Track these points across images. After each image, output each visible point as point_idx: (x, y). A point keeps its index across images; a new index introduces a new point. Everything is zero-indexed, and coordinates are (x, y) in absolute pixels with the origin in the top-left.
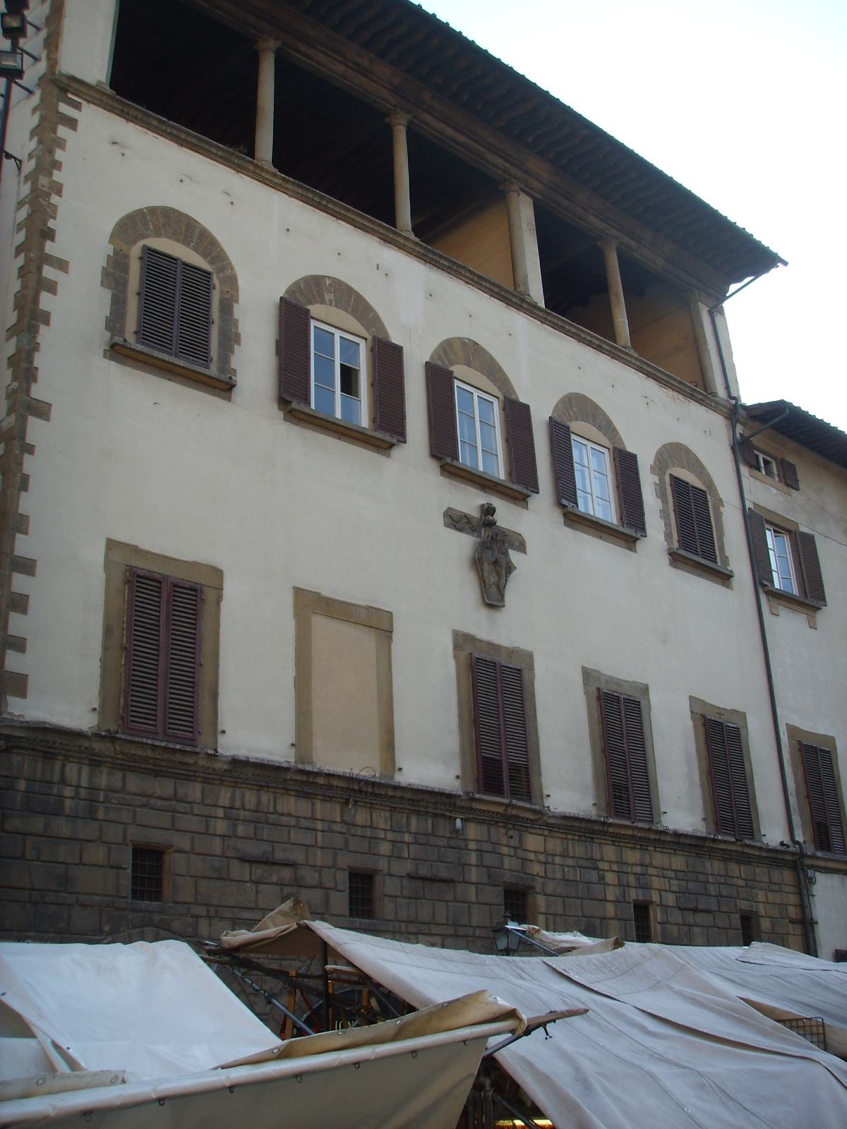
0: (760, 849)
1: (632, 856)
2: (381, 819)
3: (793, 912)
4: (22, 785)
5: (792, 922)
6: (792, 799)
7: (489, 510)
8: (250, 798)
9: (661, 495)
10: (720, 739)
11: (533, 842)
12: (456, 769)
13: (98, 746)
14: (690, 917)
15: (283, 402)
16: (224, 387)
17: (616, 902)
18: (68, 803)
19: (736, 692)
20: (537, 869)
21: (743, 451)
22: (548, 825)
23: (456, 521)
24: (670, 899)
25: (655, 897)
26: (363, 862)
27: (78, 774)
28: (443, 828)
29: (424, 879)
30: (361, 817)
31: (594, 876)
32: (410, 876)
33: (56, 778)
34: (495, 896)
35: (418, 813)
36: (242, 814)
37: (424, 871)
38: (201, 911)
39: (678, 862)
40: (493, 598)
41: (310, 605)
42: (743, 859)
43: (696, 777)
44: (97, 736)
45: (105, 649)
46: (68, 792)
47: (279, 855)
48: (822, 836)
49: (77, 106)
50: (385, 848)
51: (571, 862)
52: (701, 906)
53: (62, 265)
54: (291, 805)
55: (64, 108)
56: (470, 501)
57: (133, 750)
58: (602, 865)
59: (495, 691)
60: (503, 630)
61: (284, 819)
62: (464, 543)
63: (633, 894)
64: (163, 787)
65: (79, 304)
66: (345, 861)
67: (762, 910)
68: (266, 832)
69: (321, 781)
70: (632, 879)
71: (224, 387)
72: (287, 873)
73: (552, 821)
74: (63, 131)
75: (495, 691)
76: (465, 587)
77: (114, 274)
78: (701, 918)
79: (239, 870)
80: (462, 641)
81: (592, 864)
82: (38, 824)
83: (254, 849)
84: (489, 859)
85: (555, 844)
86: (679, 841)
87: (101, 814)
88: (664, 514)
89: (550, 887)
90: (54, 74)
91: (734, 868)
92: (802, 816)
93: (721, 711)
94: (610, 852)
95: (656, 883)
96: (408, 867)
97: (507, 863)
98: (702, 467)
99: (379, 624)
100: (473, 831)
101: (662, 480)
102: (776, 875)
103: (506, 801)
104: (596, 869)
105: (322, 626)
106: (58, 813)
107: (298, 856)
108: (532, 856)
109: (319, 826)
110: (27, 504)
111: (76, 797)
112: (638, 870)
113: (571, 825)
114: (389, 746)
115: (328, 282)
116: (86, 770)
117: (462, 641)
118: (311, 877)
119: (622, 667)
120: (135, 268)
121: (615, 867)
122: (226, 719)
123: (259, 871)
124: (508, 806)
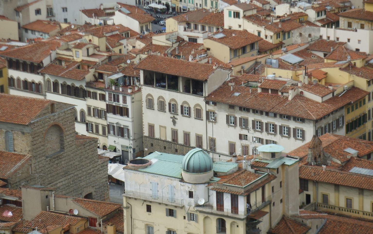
1: (187, 148)
6: (208, 145)
8: (157, 141)
9: (194, 110)
11: (178, 146)
19: (202, 132)
20: (178, 148)
23: (171, 118)
26: (165, 146)
30: (164, 143)
34: (174, 150)
41: (160, 126)
43: (195, 141)
53: (143, 101)
54: (160, 141)
56: (172, 116)
59: (175, 133)
62: (172, 120)
65: (144, 104)
75: (175, 133)
77: (146, 101)
80: (172, 129)
81: (183, 148)
85: (179, 146)
88: (194, 113)
94: (185, 147)
98: (201, 106)
99: (165, 128)
101: (194, 109)
105: (161, 128)
110: (143, 121)
117: (172, 129)
119: (187, 130)
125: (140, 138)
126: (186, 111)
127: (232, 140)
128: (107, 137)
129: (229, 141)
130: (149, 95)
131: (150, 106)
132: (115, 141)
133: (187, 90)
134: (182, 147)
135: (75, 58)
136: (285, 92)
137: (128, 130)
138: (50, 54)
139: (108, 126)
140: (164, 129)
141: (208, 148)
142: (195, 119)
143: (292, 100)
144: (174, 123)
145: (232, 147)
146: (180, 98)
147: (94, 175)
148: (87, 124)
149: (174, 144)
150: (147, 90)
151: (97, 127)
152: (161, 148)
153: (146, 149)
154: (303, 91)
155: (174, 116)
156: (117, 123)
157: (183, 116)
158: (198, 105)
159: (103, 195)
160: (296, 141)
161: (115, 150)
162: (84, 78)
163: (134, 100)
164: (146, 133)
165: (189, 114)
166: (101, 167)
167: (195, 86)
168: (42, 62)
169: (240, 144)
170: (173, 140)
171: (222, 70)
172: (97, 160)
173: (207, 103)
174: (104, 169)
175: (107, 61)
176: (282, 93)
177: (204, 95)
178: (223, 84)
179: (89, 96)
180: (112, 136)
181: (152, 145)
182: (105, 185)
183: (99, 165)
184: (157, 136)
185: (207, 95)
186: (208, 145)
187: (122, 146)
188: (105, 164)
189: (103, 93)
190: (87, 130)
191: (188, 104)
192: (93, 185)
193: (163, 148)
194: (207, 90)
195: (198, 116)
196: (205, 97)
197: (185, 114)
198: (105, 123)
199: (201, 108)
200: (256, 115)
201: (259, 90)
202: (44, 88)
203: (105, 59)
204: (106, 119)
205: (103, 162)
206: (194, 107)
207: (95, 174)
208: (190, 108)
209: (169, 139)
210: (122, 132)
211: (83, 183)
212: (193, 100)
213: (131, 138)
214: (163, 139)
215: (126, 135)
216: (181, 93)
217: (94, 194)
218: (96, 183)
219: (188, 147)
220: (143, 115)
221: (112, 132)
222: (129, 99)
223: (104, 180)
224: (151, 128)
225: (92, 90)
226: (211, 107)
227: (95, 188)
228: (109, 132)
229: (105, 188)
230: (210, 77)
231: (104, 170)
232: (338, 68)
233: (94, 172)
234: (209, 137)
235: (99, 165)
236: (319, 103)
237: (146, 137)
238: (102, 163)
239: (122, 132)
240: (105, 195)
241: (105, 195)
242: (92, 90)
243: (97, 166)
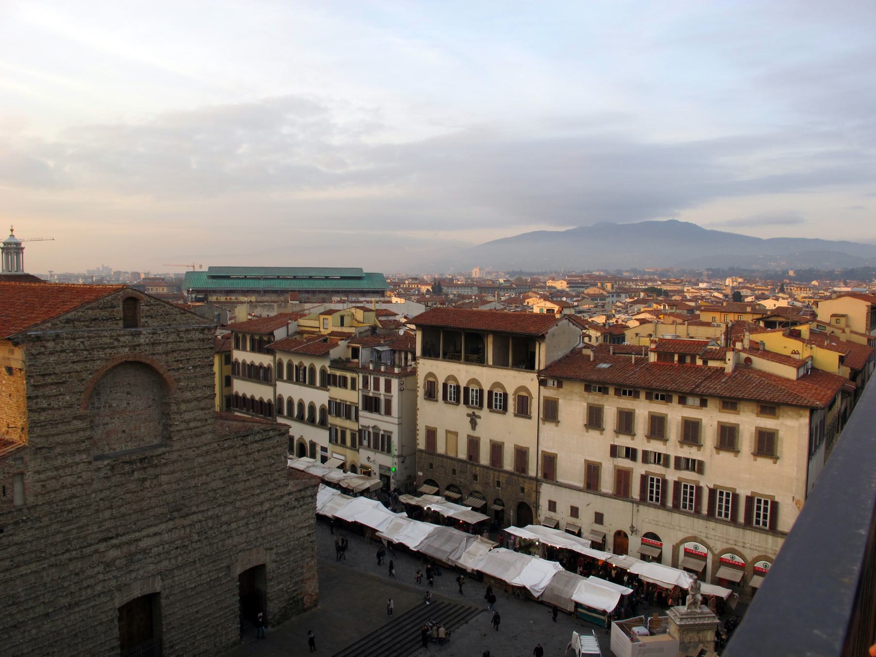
1: (497, 473)
9: (514, 400)
10: (521, 454)
11: (478, 468)
16: (437, 401)
23: (468, 415)
39: (506, 475)
41: (448, 432)
42: (523, 477)
48: (545, 476)
56: (470, 411)
59: (474, 444)
60: (475, 434)
65: (421, 392)
71: (437, 401)
75: (474, 444)
76: (469, 426)
80: (468, 436)
86: (506, 472)
88: (514, 405)
99: (456, 434)
105: (449, 435)
113: (484, 467)
117: (468, 436)
119: (498, 439)
125: (409, 455)
126: (497, 401)
128: (358, 451)
129: (586, 461)
130: (431, 374)
131: (430, 395)
132: (369, 458)
133: (501, 362)
135: (322, 330)
136: (714, 359)
138: (288, 324)
139: (360, 431)
140: (454, 437)
141: (539, 475)
142: (515, 415)
143: (734, 371)
144: (474, 425)
145: (592, 472)
146: (487, 376)
147: (273, 519)
148: (330, 429)
149: (472, 464)
150: (425, 367)
151: (343, 433)
153: (420, 474)
154: (752, 357)
155: (474, 413)
156: (374, 427)
157: (491, 411)
158: (523, 388)
159: (300, 570)
160: (755, 460)
161: (368, 473)
162: (328, 353)
163: (403, 386)
164: (422, 444)
165: (505, 409)
166: (296, 499)
167: (519, 348)
168: (272, 334)
169: (612, 467)
170: (470, 457)
171: (571, 324)
172: (283, 481)
173: (542, 383)
174: (304, 504)
175: (369, 333)
176: (705, 362)
177: (537, 368)
178: (572, 352)
179: (335, 385)
180: (365, 448)
181: (431, 466)
182: (306, 545)
183: (290, 494)
184: (441, 449)
185: (542, 368)
186: (540, 467)
187: (381, 467)
188: (309, 493)
189: (355, 375)
190: (330, 441)
191: (503, 387)
192: (268, 545)
193: (451, 473)
194: (542, 356)
195: (523, 410)
196: (540, 373)
197: (496, 407)
198: (354, 426)
199: (530, 394)
200: (654, 405)
201: (653, 358)
202: (274, 374)
203: (366, 331)
204: (357, 419)
205: (302, 487)
206: (515, 394)
207: (276, 516)
208: (505, 395)
209: (463, 455)
210: (381, 443)
211: (236, 540)
212: (513, 380)
214: (451, 454)
216: (490, 366)
217: (270, 567)
218: (277, 539)
219: (499, 471)
220: (418, 412)
221: (365, 443)
222: (395, 383)
223: (305, 532)
224: (431, 434)
225: (338, 373)
226: (548, 392)
227: (274, 551)
228: (361, 443)
229: (304, 553)
230: (550, 331)
231: (304, 507)
232: (818, 319)
233: (274, 511)
234: (543, 452)
235: (290, 494)
236: (793, 381)
237: (421, 451)
238: (300, 491)
239: (381, 443)
240: (305, 570)
241: (305, 570)
242: (338, 373)
243: (282, 496)
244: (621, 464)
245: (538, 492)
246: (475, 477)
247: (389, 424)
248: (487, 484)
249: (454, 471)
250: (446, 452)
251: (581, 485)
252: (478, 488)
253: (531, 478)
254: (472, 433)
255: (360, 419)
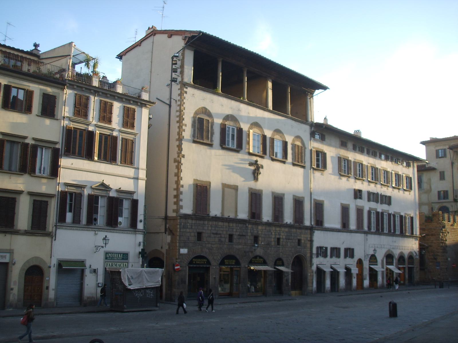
0: (304, 226)
1: (278, 229)
2: (234, 225)
3: (309, 239)
4: (182, 224)
5: (308, 241)
6: (312, 215)
7: (256, 161)
8: (214, 223)
10: (298, 203)
11: (260, 227)
12: (247, 215)
13: (193, 217)
14: (288, 241)
15: (221, 146)
17: (274, 238)
18: (189, 226)
21: (312, 135)
22: (263, 224)
24: (284, 237)
25: (281, 237)
27: (190, 221)
28: (244, 226)
29: (240, 235)
30: (231, 225)
31: (270, 233)
32: (239, 235)
33: (187, 222)
34: (252, 238)
35: (240, 223)
36: (213, 226)
37: (241, 234)
38: (206, 242)
39: (287, 230)
40: (256, 179)
42: (300, 228)
43: (292, 212)
44: (193, 215)
45: (193, 199)
46: (189, 224)
47: (218, 233)
49: (187, 88)
50: (235, 230)
51: (266, 231)
52: (290, 238)
54: (220, 224)
55: (185, 89)
57: (198, 217)
58: (272, 231)
61: (219, 226)
63: (278, 236)
64: (202, 222)
65: (188, 133)
66: (229, 233)
67: (302, 239)
68: (217, 229)
69: (225, 219)
70: (277, 234)
72: (219, 236)
73: (263, 223)
74: (185, 95)
77: (193, 126)
78: (290, 241)
79: (212, 236)
82: (185, 230)
83: (215, 232)
84: (252, 231)
85: (264, 228)
86: (287, 226)
87: (193, 228)
89: (262, 236)
90: (183, 82)
91: (298, 230)
92: (314, 219)
93: (299, 197)
94: (274, 228)
95: (282, 234)
96: (238, 233)
97: (255, 232)
100: (250, 226)
102: (306, 231)
103: (255, 220)
104: (270, 232)
106: (187, 228)
107: (221, 232)
108: (259, 230)
109: (225, 227)
111: (190, 225)
112: (279, 232)
114: (236, 212)
115: (230, 116)
116: (191, 220)
118: (223, 236)
120: (197, 121)
121: (274, 231)
122: (211, 210)
123: (215, 235)
124: (256, 221)
127: (345, 202)
129: (341, 204)
130: (205, 111)
134: (268, 228)
137: (135, 203)
140: (233, 191)
144: (256, 174)
152: (223, 239)
181: (199, 235)
193: (227, 240)
213: (140, 226)
214: (229, 214)
215: (123, 220)
234: (314, 200)
244: (359, 204)
245: (311, 241)
246: (256, 239)
247: (119, 178)
248: (268, 244)
249: (231, 237)
250: (222, 213)
251: (338, 226)
252: (259, 252)
253: (307, 228)
254: (252, 184)
255: (62, 172)
